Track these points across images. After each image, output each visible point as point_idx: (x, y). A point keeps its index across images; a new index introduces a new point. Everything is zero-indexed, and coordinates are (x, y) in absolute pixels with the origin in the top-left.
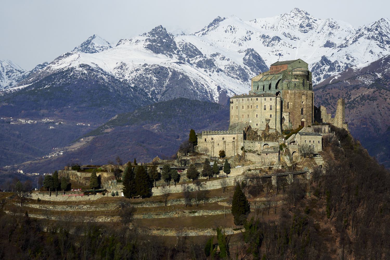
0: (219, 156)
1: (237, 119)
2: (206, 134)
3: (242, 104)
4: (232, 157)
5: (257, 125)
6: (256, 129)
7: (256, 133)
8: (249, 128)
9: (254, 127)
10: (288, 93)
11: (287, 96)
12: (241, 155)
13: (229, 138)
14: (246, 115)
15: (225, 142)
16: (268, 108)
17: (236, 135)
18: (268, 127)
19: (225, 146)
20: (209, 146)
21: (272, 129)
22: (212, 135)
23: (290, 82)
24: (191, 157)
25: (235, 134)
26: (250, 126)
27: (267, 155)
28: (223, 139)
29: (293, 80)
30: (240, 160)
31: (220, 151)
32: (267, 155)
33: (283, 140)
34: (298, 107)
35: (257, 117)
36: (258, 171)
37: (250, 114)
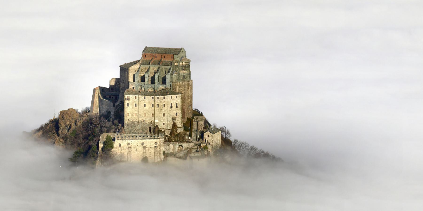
1: (136, 117)
2: (120, 138)
3: (143, 102)
5: (164, 124)
6: (163, 128)
13: (150, 143)
15: (145, 147)
16: (174, 106)
18: (174, 125)
20: (125, 152)
22: (128, 139)
23: (179, 74)
25: (158, 139)
26: (157, 126)
28: (143, 144)
29: (181, 71)
35: (164, 115)
37: (156, 113)
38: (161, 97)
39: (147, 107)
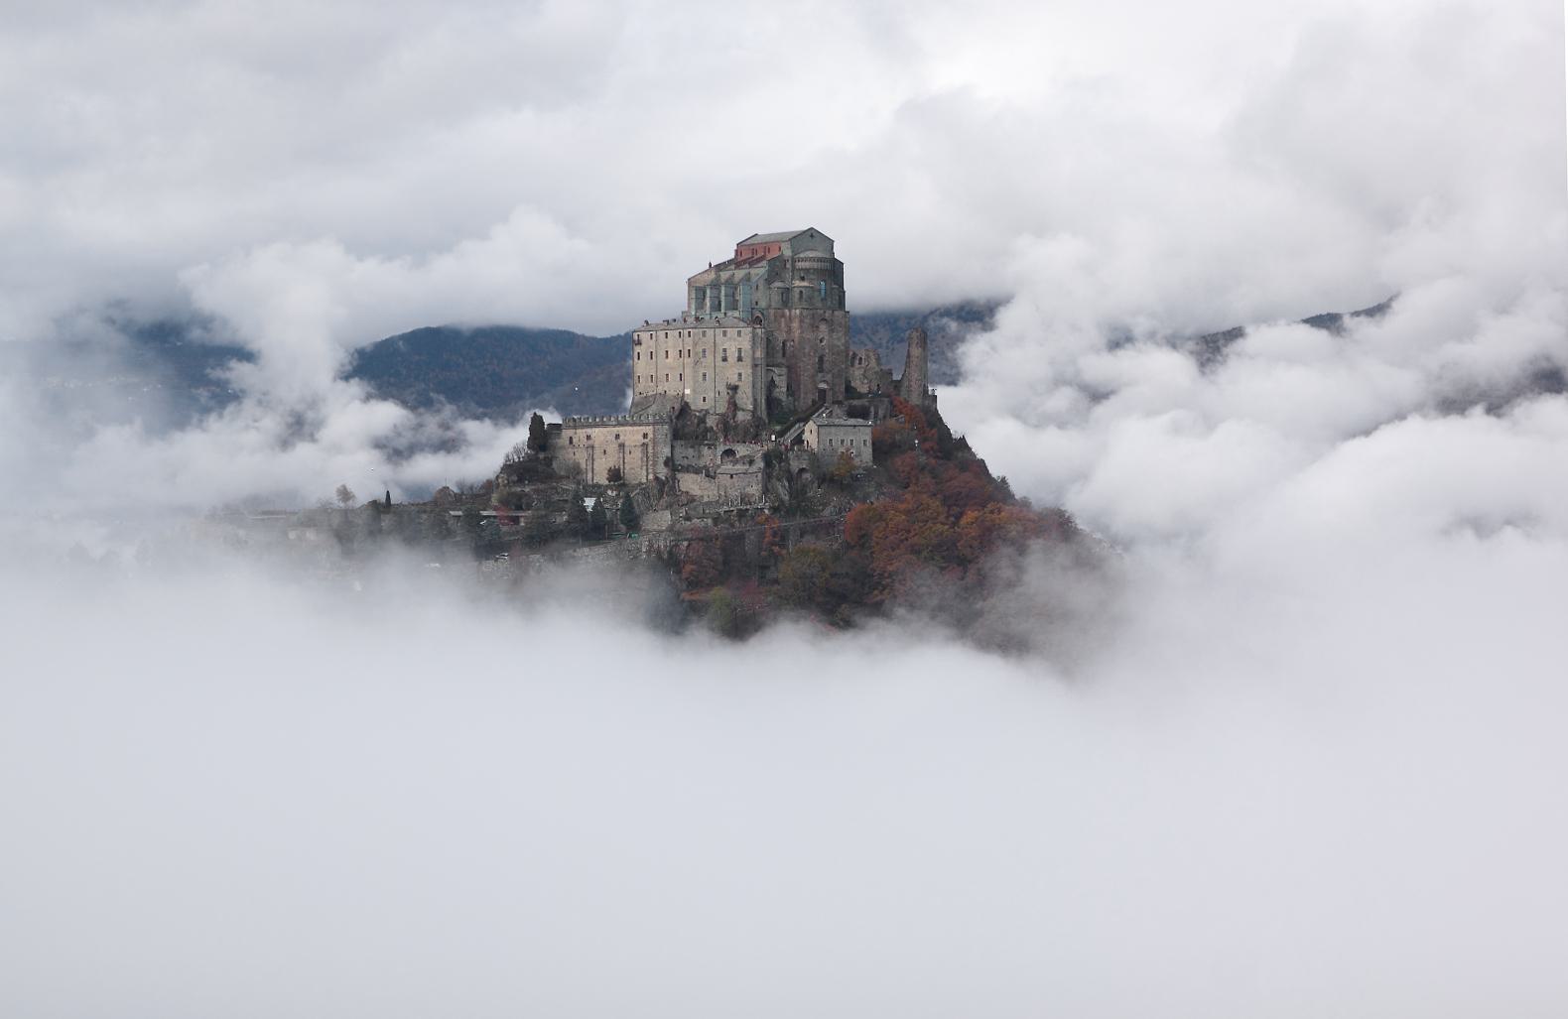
0: (607, 482)
4: (641, 484)
7: (702, 420)
8: (684, 409)
9: (697, 405)
10: (783, 316)
11: (780, 323)
12: (664, 478)
14: (674, 376)
16: (732, 355)
17: (651, 427)
18: (734, 406)
19: (621, 455)
20: (581, 457)
21: (743, 410)
24: (536, 487)
25: (648, 424)
27: (732, 477)
28: (617, 436)
29: (797, 283)
30: (661, 492)
31: (610, 470)
32: (732, 477)
33: (773, 437)
34: (809, 352)
36: (710, 521)
37: (688, 372)
38: (697, 330)
39: (670, 360)
